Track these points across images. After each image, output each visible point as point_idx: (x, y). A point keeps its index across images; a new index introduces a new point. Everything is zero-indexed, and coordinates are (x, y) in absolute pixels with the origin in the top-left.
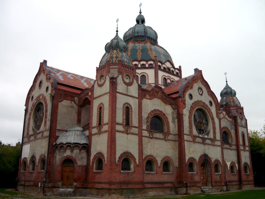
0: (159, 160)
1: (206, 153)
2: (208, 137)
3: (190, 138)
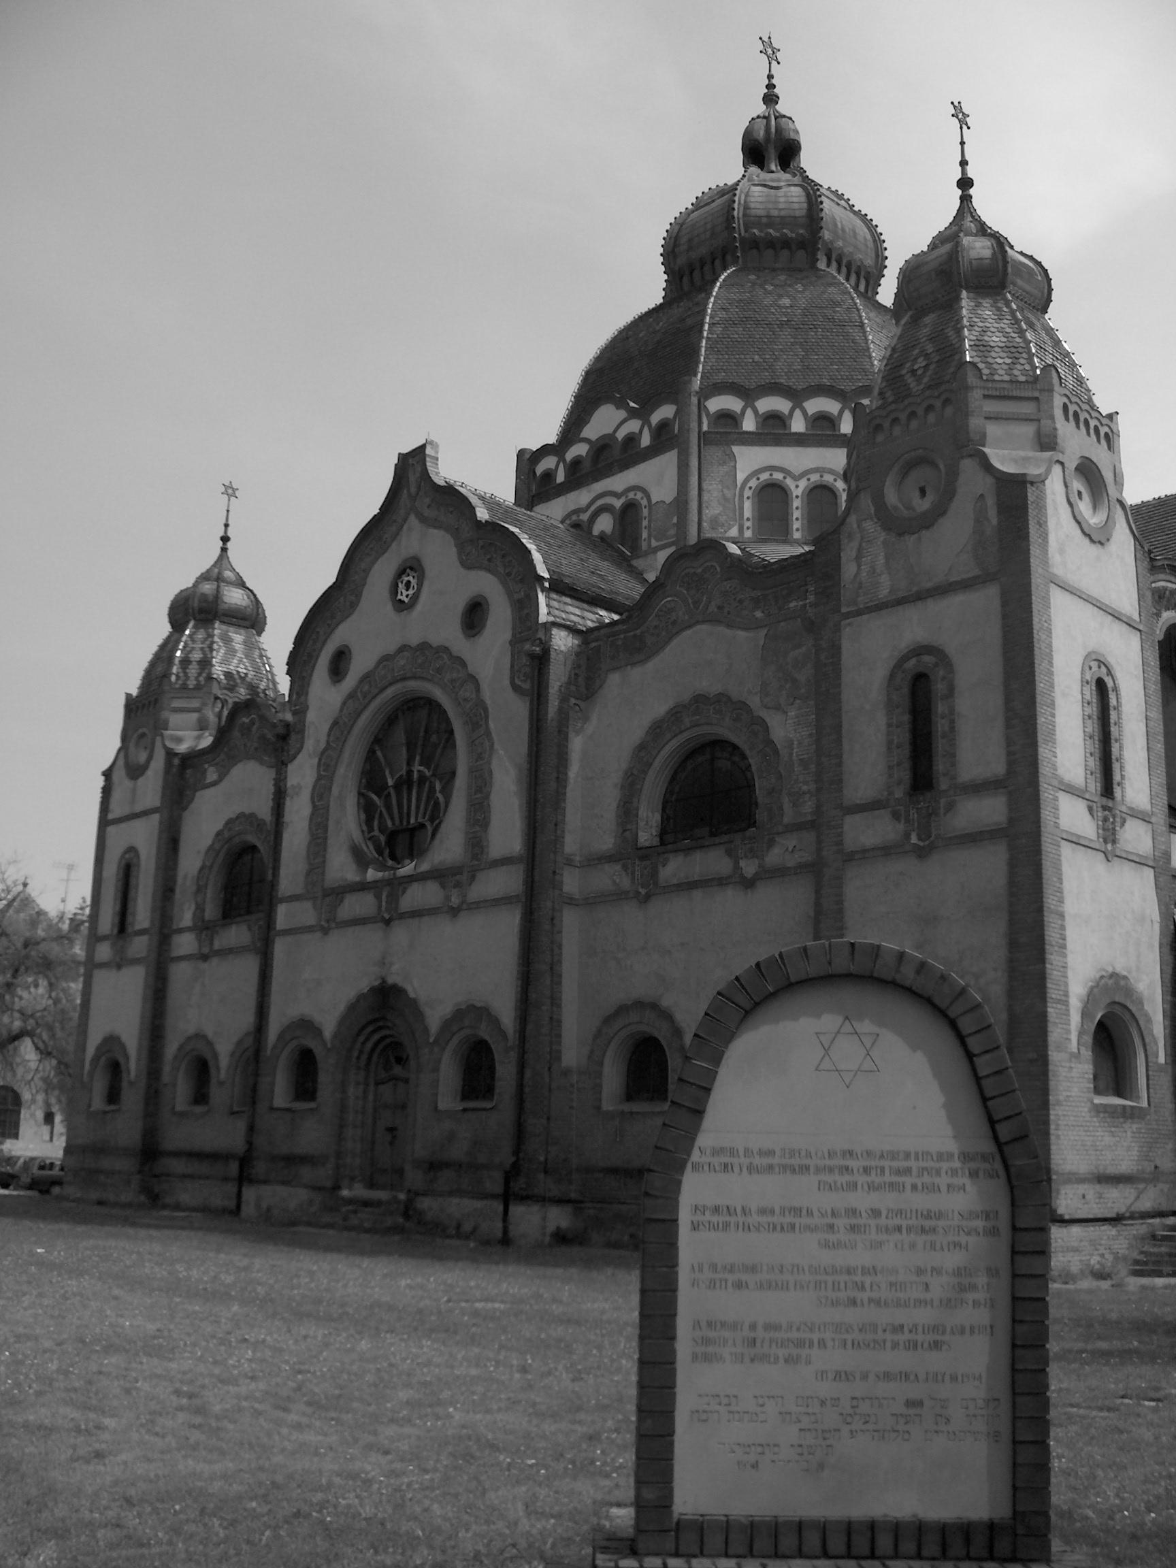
0: (224, 1050)
1: (391, 980)
2: (425, 867)
3: (305, 914)
